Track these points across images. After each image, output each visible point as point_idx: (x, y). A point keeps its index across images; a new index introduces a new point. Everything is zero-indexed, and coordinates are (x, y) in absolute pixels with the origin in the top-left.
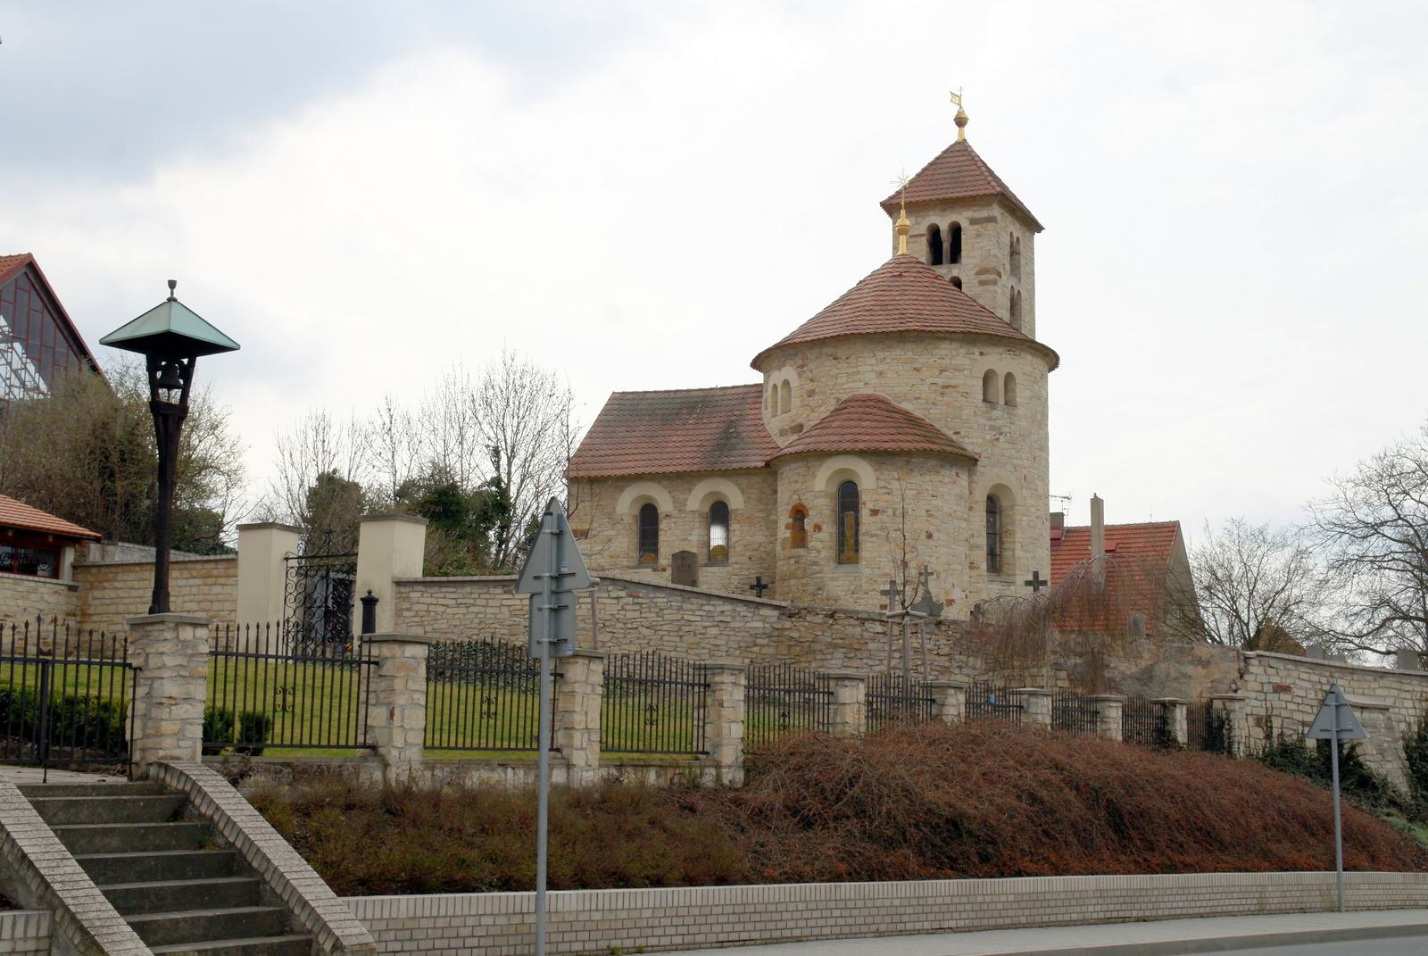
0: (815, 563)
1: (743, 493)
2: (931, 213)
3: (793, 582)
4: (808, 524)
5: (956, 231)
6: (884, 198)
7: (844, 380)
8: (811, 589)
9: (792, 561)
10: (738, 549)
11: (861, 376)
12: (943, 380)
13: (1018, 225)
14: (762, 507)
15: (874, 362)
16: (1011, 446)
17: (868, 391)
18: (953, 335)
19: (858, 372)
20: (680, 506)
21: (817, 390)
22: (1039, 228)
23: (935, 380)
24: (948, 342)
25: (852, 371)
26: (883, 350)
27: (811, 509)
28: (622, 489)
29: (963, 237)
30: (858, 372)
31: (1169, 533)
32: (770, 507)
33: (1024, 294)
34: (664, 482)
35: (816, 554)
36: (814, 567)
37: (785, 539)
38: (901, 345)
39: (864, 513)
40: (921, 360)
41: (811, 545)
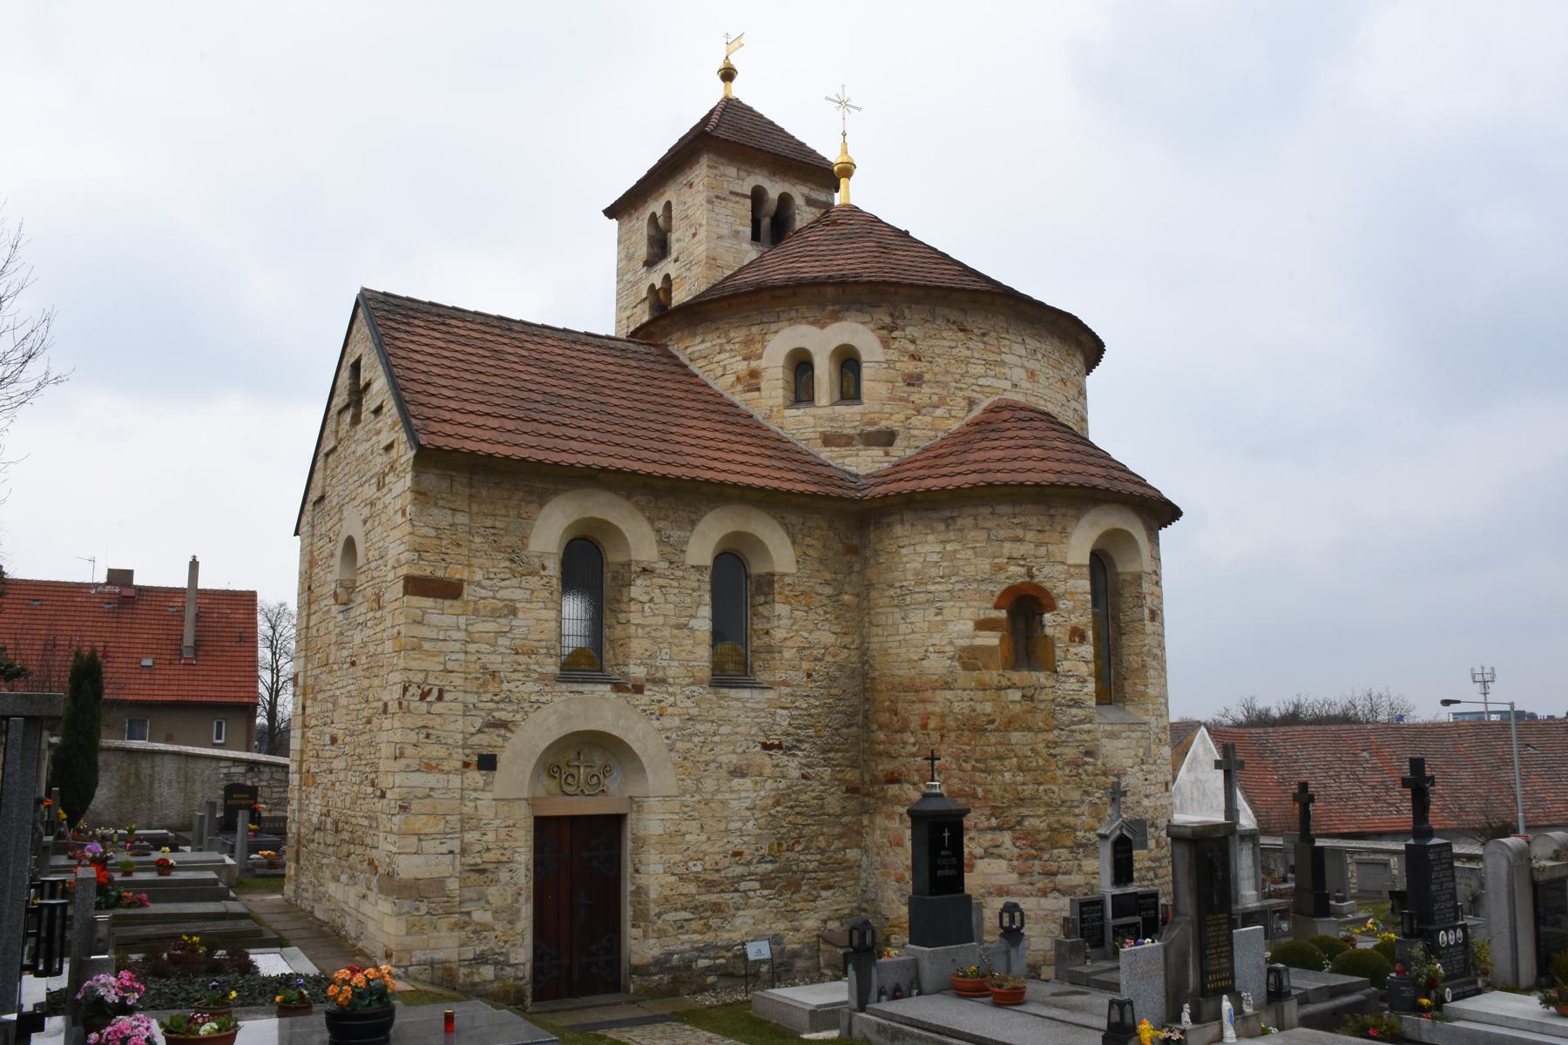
0: (1077, 703)
1: (794, 543)
3: (1016, 736)
4: (1052, 624)
8: (1070, 752)
9: (1016, 695)
10: (787, 654)
15: (1023, 353)
17: (1019, 398)
20: (673, 551)
21: (927, 377)
25: (993, 357)
27: (1061, 596)
28: (542, 500)
31: (249, 599)
32: (840, 577)
35: (1077, 686)
36: (1074, 711)
41: (1064, 666)
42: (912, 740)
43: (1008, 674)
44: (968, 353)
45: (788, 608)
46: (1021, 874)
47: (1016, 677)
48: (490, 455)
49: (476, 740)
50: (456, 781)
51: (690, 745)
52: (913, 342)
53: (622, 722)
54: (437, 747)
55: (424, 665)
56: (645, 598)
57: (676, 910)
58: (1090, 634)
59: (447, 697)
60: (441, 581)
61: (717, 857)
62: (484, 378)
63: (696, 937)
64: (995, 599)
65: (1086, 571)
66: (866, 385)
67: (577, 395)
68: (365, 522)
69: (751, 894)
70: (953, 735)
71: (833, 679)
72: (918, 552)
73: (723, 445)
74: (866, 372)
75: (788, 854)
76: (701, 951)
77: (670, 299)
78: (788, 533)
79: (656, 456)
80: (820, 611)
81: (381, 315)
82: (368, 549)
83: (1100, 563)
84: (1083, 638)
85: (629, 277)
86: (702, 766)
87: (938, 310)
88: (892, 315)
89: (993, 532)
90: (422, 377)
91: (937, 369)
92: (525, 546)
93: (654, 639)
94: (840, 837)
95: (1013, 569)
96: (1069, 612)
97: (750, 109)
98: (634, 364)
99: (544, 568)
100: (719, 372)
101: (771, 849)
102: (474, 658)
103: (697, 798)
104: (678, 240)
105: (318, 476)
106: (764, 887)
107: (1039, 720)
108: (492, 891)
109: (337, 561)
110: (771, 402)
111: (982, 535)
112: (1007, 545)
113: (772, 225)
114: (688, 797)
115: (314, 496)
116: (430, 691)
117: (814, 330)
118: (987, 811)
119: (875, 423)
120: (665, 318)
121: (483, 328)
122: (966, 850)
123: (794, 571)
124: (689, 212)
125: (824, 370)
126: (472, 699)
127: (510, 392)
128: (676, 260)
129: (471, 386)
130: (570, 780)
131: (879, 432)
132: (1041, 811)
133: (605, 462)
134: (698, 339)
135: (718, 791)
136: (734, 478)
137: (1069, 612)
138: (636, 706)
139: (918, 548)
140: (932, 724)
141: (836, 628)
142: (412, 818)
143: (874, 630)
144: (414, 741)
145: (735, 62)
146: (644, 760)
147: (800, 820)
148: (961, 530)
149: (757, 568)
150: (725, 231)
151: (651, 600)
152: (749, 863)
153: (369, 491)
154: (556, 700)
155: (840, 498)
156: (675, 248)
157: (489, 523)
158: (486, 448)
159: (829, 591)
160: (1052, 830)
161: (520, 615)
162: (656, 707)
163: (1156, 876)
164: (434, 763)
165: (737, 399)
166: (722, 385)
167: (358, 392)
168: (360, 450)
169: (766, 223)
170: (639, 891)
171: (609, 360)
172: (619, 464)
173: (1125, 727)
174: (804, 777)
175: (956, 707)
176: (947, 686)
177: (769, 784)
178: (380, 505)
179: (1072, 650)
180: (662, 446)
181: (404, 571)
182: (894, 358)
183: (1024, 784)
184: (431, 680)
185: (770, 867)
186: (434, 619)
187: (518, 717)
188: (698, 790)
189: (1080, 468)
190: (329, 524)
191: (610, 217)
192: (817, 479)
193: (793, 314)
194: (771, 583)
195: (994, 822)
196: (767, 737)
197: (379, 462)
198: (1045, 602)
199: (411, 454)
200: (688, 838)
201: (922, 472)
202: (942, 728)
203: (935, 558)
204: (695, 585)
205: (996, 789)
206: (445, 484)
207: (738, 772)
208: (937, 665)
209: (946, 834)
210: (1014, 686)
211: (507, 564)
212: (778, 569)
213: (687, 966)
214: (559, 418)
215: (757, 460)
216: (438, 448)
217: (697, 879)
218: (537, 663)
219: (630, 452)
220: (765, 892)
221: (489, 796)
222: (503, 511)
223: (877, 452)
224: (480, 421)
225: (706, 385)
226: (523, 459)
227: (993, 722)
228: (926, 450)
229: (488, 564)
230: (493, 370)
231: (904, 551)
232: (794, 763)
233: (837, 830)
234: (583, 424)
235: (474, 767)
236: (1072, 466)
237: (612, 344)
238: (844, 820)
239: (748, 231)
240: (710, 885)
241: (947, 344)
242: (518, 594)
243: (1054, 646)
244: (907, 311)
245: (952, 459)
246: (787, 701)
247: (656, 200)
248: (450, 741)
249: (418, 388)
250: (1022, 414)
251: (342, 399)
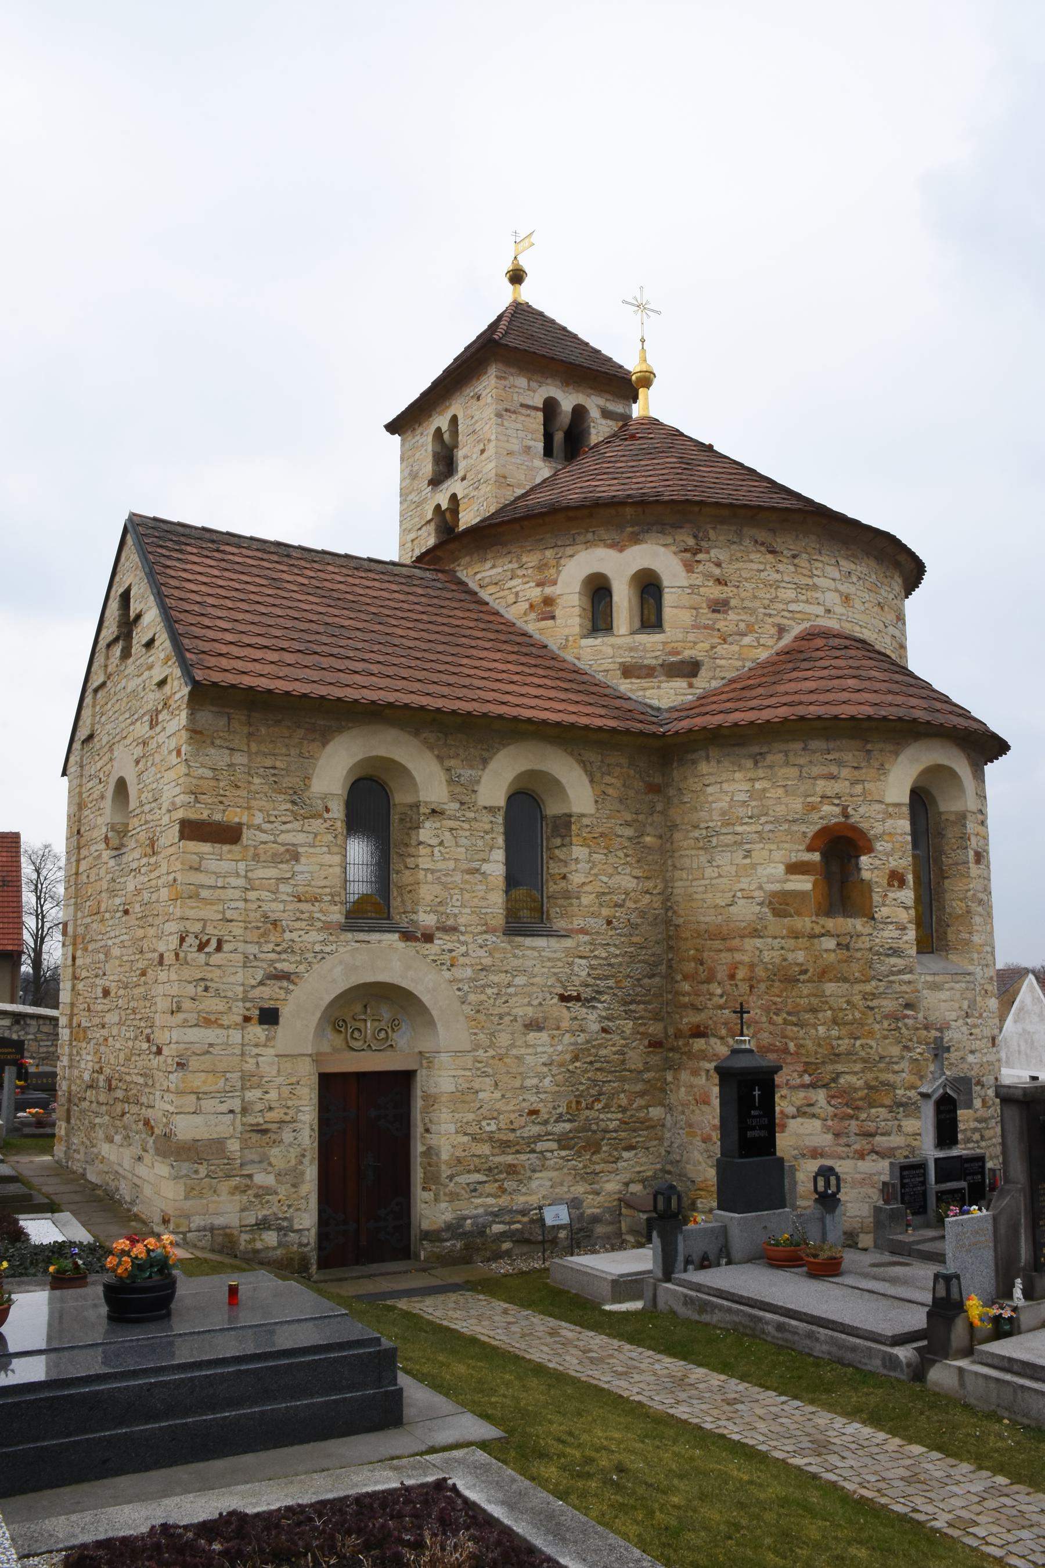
0: (896, 952)
1: (592, 781)
2: (549, 381)
3: (830, 988)
8: (889, 1005)
9: (830, 943)
10: (585, 900)
14: (629, 817)
15: (837, 575)
17: (832, 624)
19: (815, 587)
20: (464, 792)
21: (733, 603)
26: (847, 558)
28: (325, 737)
30: (815, 587)
32: (641, 817)
35: (896, 934)
36: (893, 960)
38: (865, 558)
40: (882, 591)
42: (719, 991)
43: (822, 921)
44: (778, 577)
45: (586, 850)
46: (837, 1135)
47: (830, 923)
48: (269, 691)
49: (256, 993)
50: (236, 1036)
51: (483, 997)
52: (718, 565)
53: (411, 973)
54: (217, 1000)
55: (202, 914)
56: (434, 841)
57: (469, 1172)
58: (910, 878)
59: (226, 947)
60: (218, 824)
61: (512, 1116)
62: (263, 609)
63: (490, 1201)
64: (807, 841)
65: (906, 810)
66: (668, 613)
67: (360, 625)
68: (137, 762)
69: (548, 1155)
70: (763, 986)
71: (636, 926)
72: (725, 790)
73: (516, 678)
74: (669, 598)
75: (587, 1112)
76: (496, 1215)
77: (457, 519)
78: (586, 771)
79: (446, 690)
80: (621, 854)
81: (152, 541)
82: (141, 791)
83: (921, 801)
84: (902, 883)
85: (413, 497)
86: (496, 1019)
87: (745, 530)
88: (695, 537)
89: (805, 770)
90: (196, 608)
91: (743, 595)
92: (308, 787)
93: (444, 885)
94: (642, 1094)
95: (826, 808)
96: (888, 855)
97: (541, 314)
98: (420, 591)
99: (327, 810)
100: (511, 599)
101: (569, 1107)
102: (254, 906)
103: (491, 1053)
104: (465, 457)
105: (86, 713)
106: (562, 1148)
107: (855, 970)
108: (275, 1151)
109: (108, 803)
110: (567, 631)
111: (794, 772)
112: (821, 783)
113: (566, 440)
114: (481, 1052)
115: (83, 734)
116: (208, 941)
117: (612, 553)
118: (800, 1068)
119: (678, 653)
120: (453, 542)
121: (259, 554)
122: (777, 1109)
123: (592, 811)
124: (477, 427)
125: (623, 597)
126: (252, 949)
127: (289, 624)
128: (463, 479)
129: (248, 617)
130: (356, 1034)
131: (682, 662)
132: (858, 1067)
133: (391, 697)
134: (489, 564)
135: (513, 1046)
136: (527, 713)
137: (888, 855)
138: (425, 956)
139: (725, 786)
140: (741, 974)
141: (638, 873)
142: (190, 1075)
143: (678, 874)
144: (192, 994)
145: (524, 263)
146: (435, 1013)
147: (600, 1076)
148: (771, 767)
149: (553, 809)
150: (515, 446)
151: (441, 843)
152: (546, 1122)
153: (142, 729)
154: (341, 950)
155: (642, 733)
156: (462, 466)
157: (268, 763)
158: (264, 683)
159: (629, 832)
160: (870, 1087)
161: (303, 860)
162: (447, 957)
163: (982, 1138)
164: (213, 1017)
165: (531, 628)
166: (514, 613)
167: (128, 624)
168: (132, 685)
169: (559, 437)
170: (430, 1152)
171: (395, 587)
172: (406, 699)
173: (948, 978)
174: (604, 1030)
175: (767, 956)
176: (756, 933)
177: (567, 1038)
178: (153, 744)
179: (891, 895)
180: (452, 679)
181: (180, 814)
182: (698, 582)
183: (839, 1038)
184: (210, 930)
185: (568, 1126)
186: (212, 865)
187: (301, 968)
188: (492, 1045)
189: (899, 699)
190: (99, 765)
191: (393, 433)
192: (616, 713)
193: (590, 536)
194: (568, 825)
195: (807, 1079)
196: (565, 988)
197: (152, 698)
198: (861, 843)
199: (189, 688)
200: (481, 1095)
201: (729, 705)
202: (751, 979)
203: (743, 797)
204: (488, 827)
205: (809, 1043)
206: (222, 722)
207: (534, 1026)
208: (745, 912)
209: (757, 1093)
210: (828, 934)
211: (289, 806)
212: (576, 809)
213: (481, 1231)
214: (341, 651)
215: (552, 694)
216: (215, 684)
217: (491, 1139)
218: (321, 911)
219: (417, 686)
220: (563, 1153)
221: (271, 1051)
222: (284, 751)
223: (681, 684)
224: (258, 654)
225: (497, 613)
226: (305, 695)
227: (805, 972)
228: (732, 681)
229: (268, 806)
230: (271, 600)
231: (709, 790)
232: (593, 1016)
233: (639, 1087)
234: (367, 656)
235: (255, 1021)
236: (890, 698)
237: (397, 570)
238: (647, 1076)
239: (540, 446)
240: (505, 1146)
241: (755, 566)
242: (300, 838)
243: (871, 891)
244: (712, 534)
245: (761, 691)
246: (585, 950)
247: (440, 414)
248: (230, 994)
249: (192, 619)
250: (836, 642)
251: (111, 631)
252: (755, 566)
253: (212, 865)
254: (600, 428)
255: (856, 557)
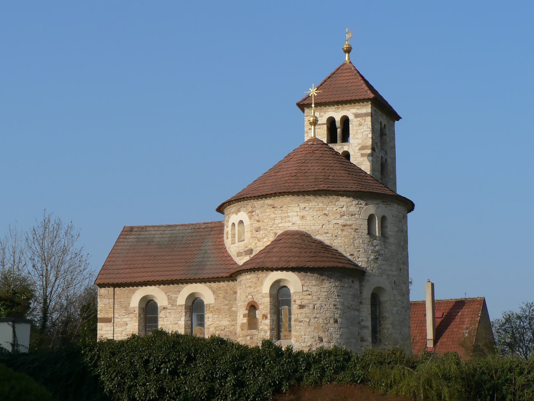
4: (259, 314)
5: (345, 121)
6: (299, 100)
7: (279, 221)
9: (248, 338)
11: (290, 219)
12: (342, 221)
13: (384, 117)
16: (385, 262)
17: (295, 228)
18: (348, 193)
20: (172, 301)
21: (261, 227)
22: (398, 118)
23: (338, 221)
24: (345, 197)
29: (350, 125)
33: (389, 161)
34: (162, 286)
37: (243, 324)
39: (294, 307)
41: (260, 327)
45: (211, 314)
47: (249, 332)
52: (258, 215)
58: (269, 316)
78: (212, 291)
80: (224, 314)
84: (266, 318)
92: (129, 305)
159: (227, 307)
204: (180, 311)
241: (268, 214)
244: (256, 205)
252: (268, 214)
253: (104, 328)
254: (354, 123)
255: (310, 201)
